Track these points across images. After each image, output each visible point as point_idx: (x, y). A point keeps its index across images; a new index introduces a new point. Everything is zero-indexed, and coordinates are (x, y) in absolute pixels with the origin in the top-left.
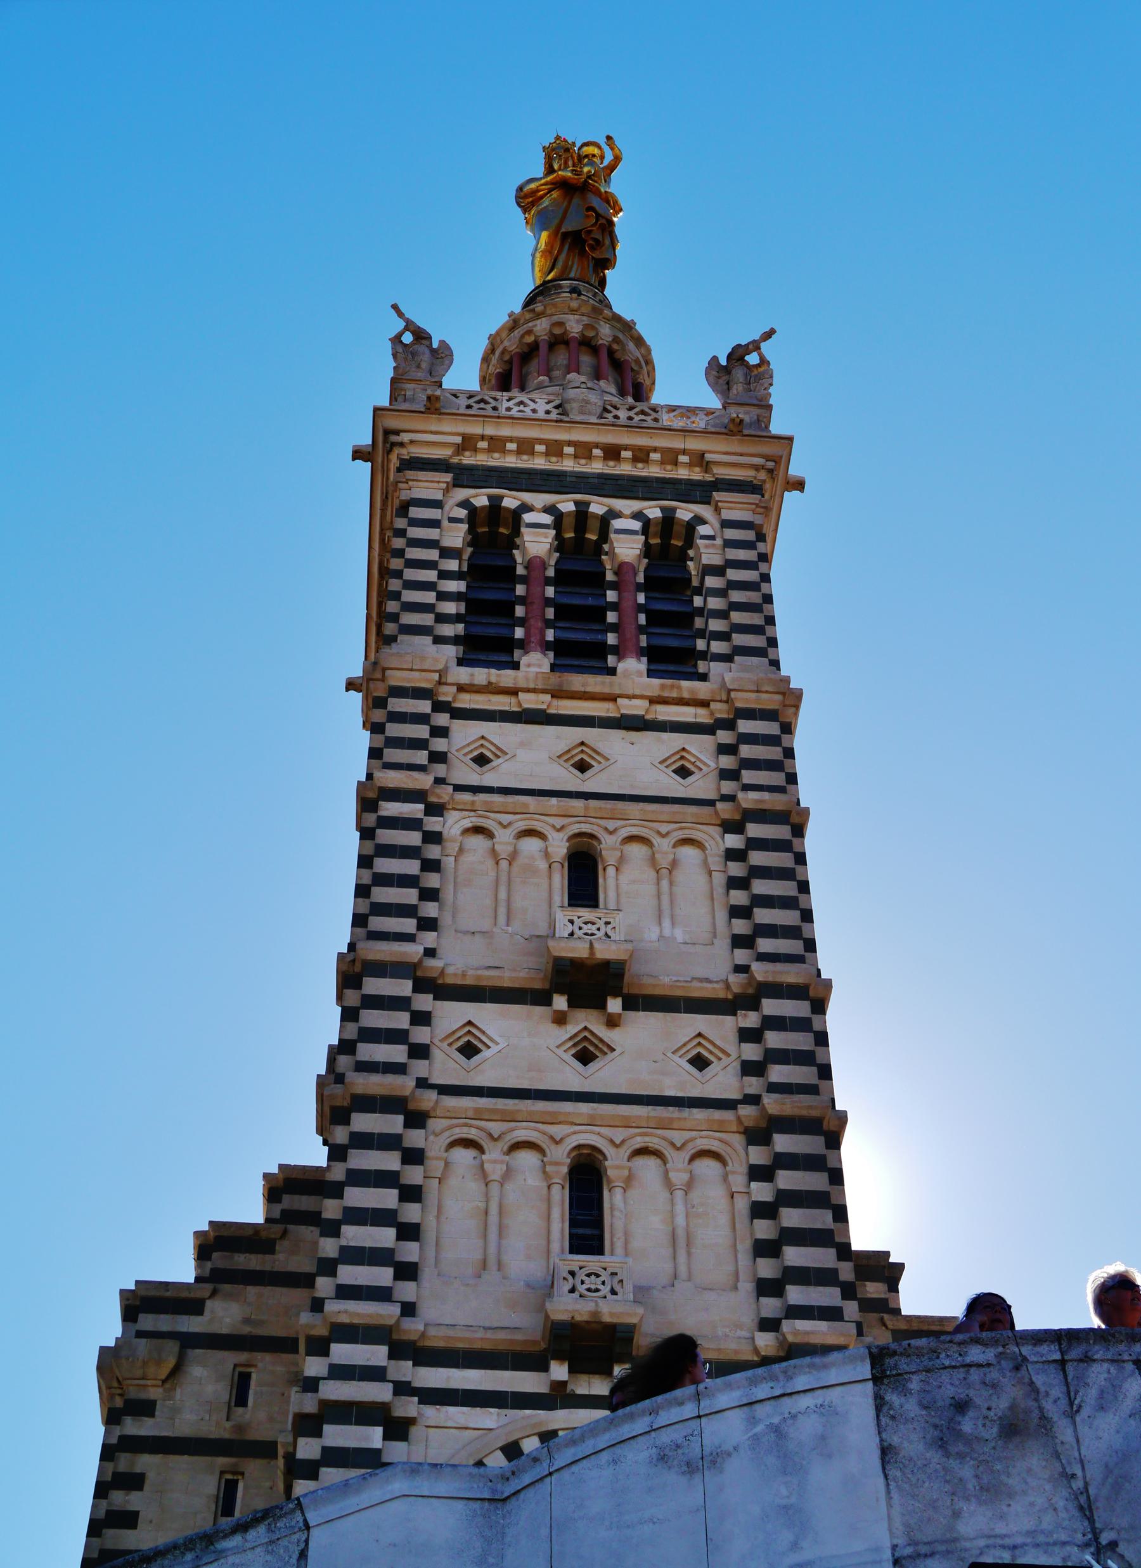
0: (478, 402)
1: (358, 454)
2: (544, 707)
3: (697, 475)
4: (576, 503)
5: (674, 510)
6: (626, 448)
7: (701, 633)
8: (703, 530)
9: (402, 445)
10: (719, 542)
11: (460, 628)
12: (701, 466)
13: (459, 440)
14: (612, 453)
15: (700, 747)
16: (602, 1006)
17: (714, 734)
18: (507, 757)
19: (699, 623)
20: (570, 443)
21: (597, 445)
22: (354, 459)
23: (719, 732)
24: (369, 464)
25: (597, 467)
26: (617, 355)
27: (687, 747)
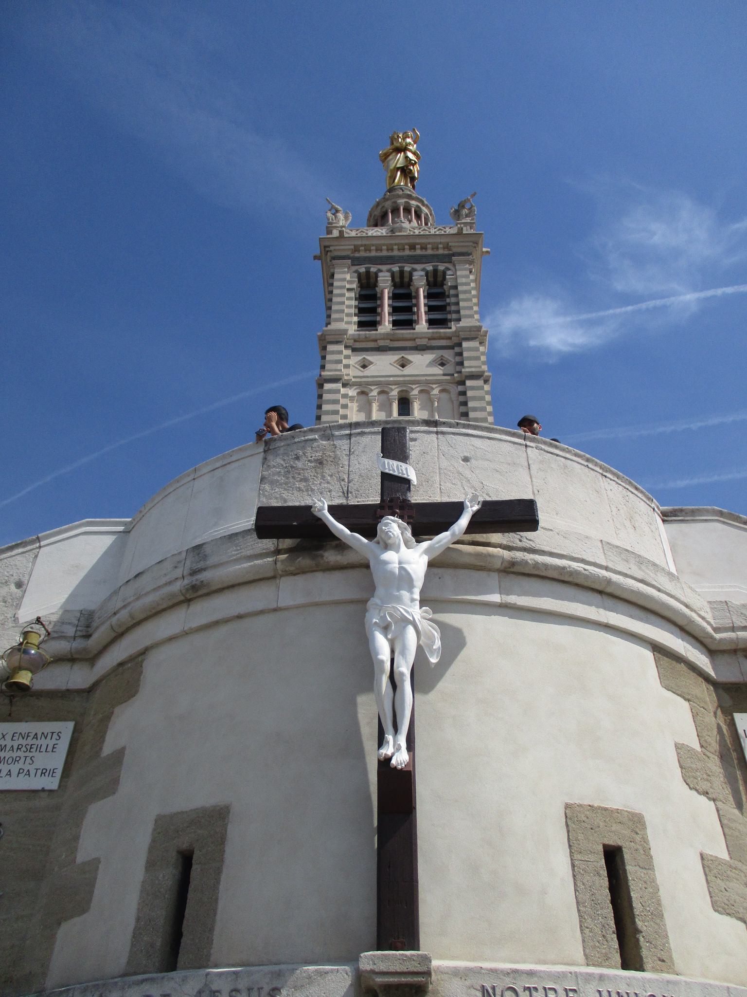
0: (361, 232)
1: (315, 258)
2: (387, 344)
3: (446, 252)
4: (399, 267)
5: (438, 266)
6: (418, 244)
7: (450, 312)
8: (449, 272)
9: (331, 251)
11: (356, 319)
12: (448, 248)
13: (352, 247)
14: (412, 247)
15: (448, 355)
17: (454, 349)
18: (374, 364)
19: (448, 308)
20: (396, 244)
21: (406, 244)
22: (314, 259)
23: (455, 348)
24: (320, 261)
25: (407, 252)
26: (418, 213)
27: (444, 355)
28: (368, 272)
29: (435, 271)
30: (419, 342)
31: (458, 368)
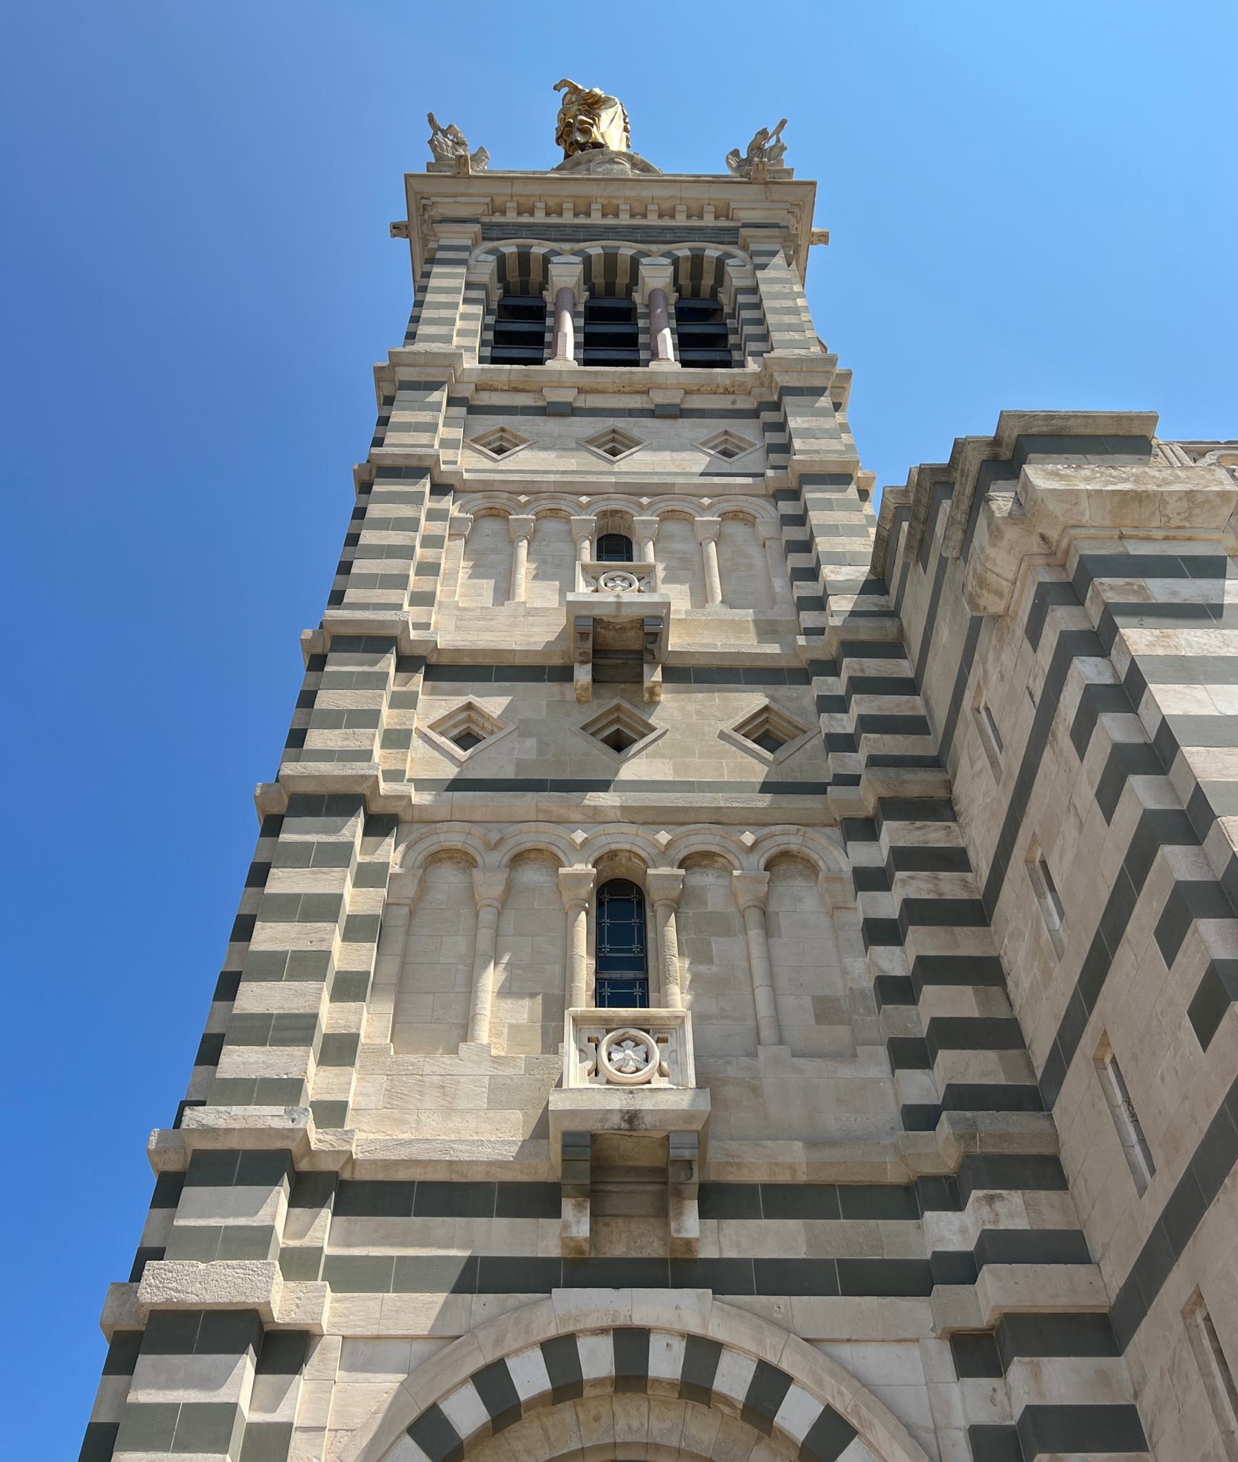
3: (723, 223)
10: (749, 267)
12: (727, 218)
13: (488, 200)
16: (639, 679)
17: (758, 417)
19: (732, 339)
23: (762, 414)
24: (408, 239)
27: (730, 430)
28: (524, 257)
29: (697, 260)
30: (659, 398)
31: (776, 458)
